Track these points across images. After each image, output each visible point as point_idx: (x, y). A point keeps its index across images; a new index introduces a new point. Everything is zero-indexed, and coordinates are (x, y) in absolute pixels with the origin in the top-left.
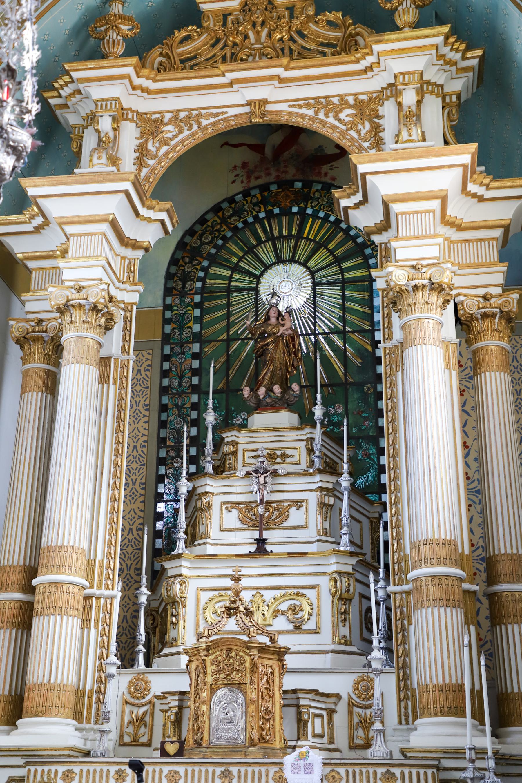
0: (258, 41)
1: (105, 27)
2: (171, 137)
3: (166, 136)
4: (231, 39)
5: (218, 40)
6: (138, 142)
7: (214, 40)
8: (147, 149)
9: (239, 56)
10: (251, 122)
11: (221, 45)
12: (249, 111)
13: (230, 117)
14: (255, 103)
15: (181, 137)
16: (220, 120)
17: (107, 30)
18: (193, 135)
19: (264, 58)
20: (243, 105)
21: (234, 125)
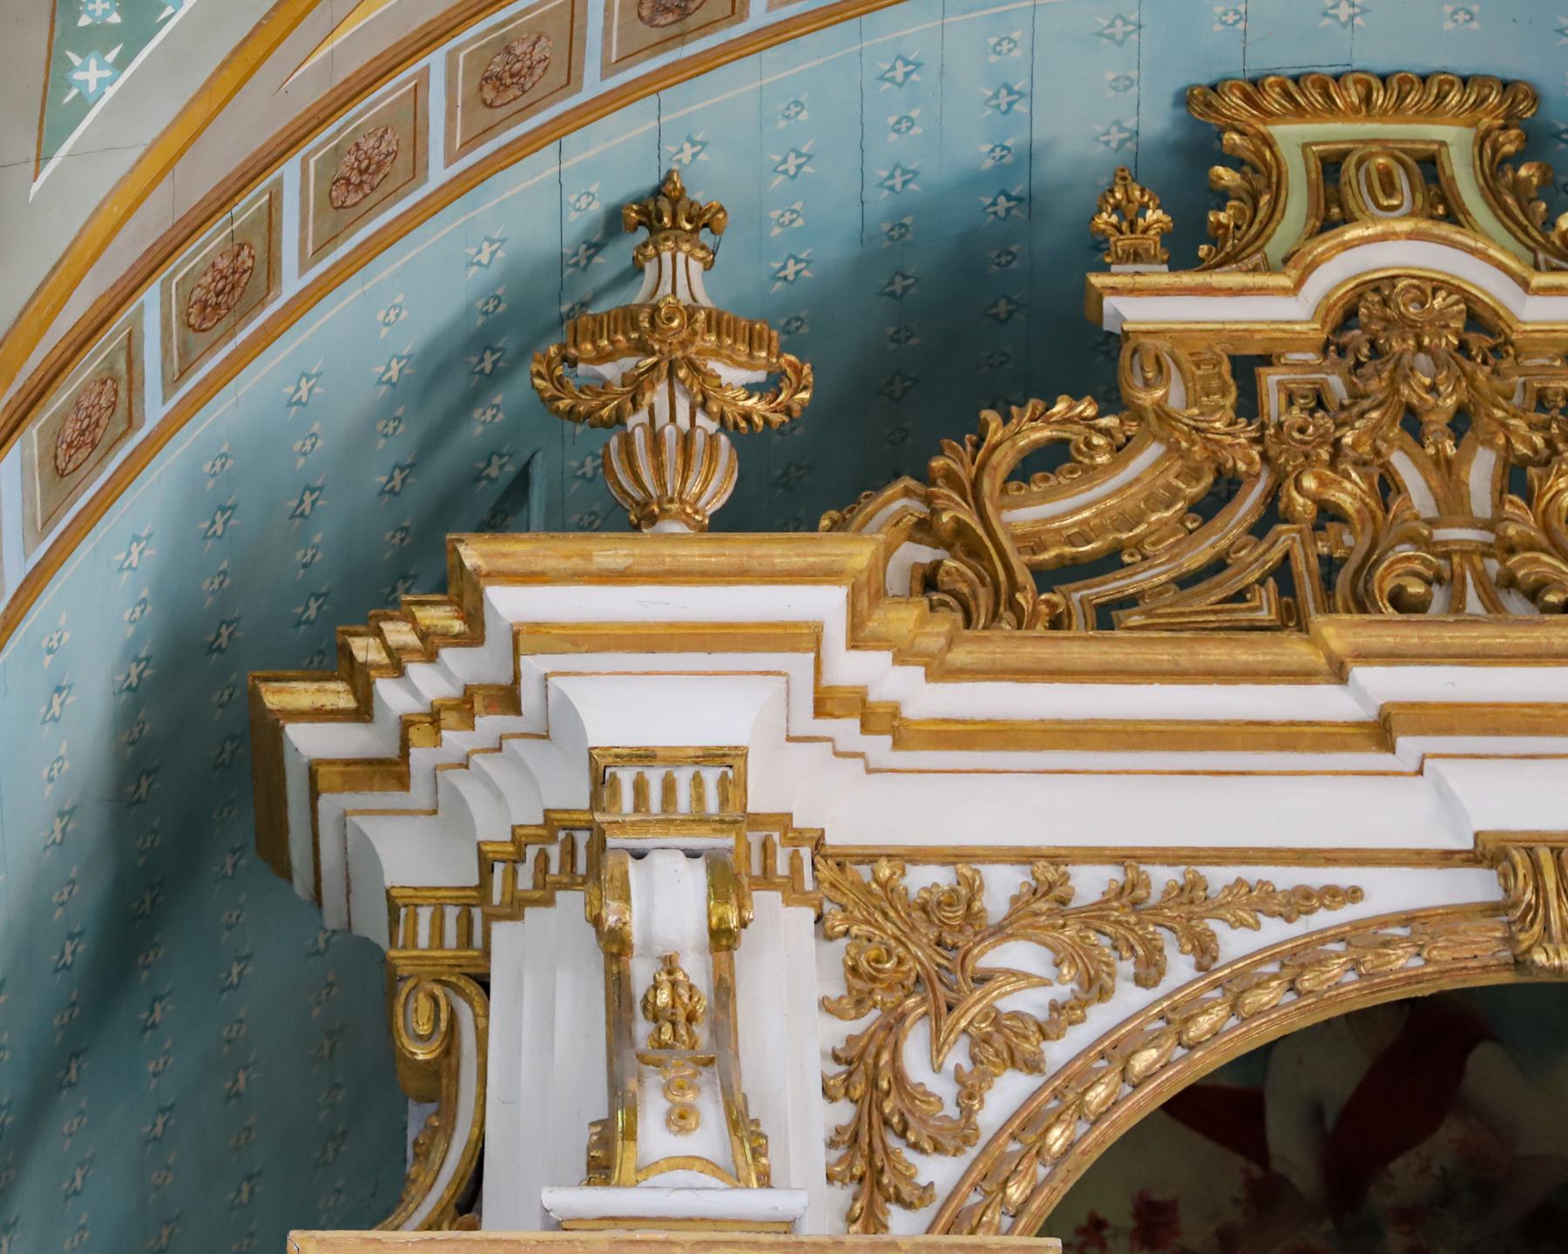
0: (1453, 503)
1: (628, 363)
2: (1042, 1015)
3: (1007, 1005)
4: (1309, 483)
5: (1226, 488)
6: (839, 1031)
7: (1208, 479)
8: (899, 1079)
9: (1384, 581)
10: (1520, 963)
11: (1249, 503)
12: (1497, 895)
13: (1384, 921)
14: (1530, 852)
15: (1100, 1019)
16: (1323, 936)
17: (636, 387)
18: (1176, 1017)
19: (1515, 604)
20: (1446, 858)
21: (1418, 979)
